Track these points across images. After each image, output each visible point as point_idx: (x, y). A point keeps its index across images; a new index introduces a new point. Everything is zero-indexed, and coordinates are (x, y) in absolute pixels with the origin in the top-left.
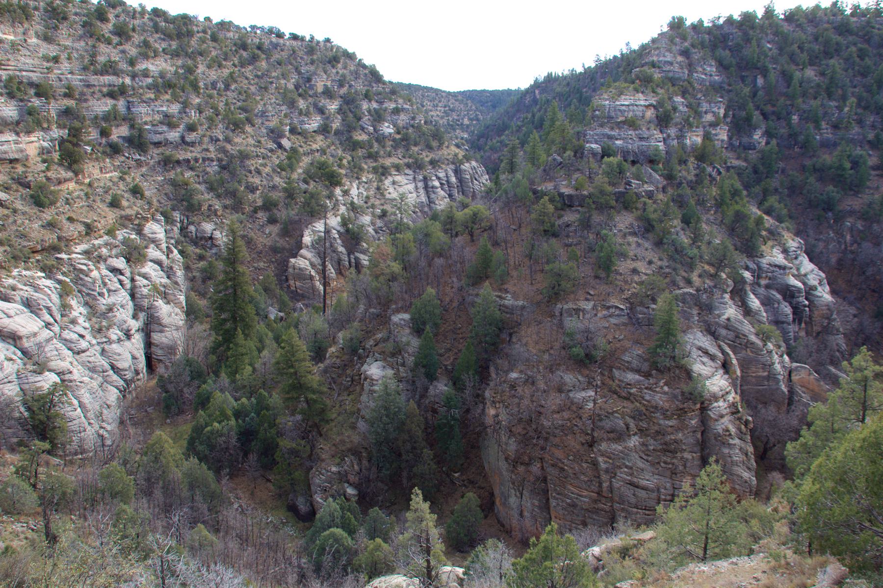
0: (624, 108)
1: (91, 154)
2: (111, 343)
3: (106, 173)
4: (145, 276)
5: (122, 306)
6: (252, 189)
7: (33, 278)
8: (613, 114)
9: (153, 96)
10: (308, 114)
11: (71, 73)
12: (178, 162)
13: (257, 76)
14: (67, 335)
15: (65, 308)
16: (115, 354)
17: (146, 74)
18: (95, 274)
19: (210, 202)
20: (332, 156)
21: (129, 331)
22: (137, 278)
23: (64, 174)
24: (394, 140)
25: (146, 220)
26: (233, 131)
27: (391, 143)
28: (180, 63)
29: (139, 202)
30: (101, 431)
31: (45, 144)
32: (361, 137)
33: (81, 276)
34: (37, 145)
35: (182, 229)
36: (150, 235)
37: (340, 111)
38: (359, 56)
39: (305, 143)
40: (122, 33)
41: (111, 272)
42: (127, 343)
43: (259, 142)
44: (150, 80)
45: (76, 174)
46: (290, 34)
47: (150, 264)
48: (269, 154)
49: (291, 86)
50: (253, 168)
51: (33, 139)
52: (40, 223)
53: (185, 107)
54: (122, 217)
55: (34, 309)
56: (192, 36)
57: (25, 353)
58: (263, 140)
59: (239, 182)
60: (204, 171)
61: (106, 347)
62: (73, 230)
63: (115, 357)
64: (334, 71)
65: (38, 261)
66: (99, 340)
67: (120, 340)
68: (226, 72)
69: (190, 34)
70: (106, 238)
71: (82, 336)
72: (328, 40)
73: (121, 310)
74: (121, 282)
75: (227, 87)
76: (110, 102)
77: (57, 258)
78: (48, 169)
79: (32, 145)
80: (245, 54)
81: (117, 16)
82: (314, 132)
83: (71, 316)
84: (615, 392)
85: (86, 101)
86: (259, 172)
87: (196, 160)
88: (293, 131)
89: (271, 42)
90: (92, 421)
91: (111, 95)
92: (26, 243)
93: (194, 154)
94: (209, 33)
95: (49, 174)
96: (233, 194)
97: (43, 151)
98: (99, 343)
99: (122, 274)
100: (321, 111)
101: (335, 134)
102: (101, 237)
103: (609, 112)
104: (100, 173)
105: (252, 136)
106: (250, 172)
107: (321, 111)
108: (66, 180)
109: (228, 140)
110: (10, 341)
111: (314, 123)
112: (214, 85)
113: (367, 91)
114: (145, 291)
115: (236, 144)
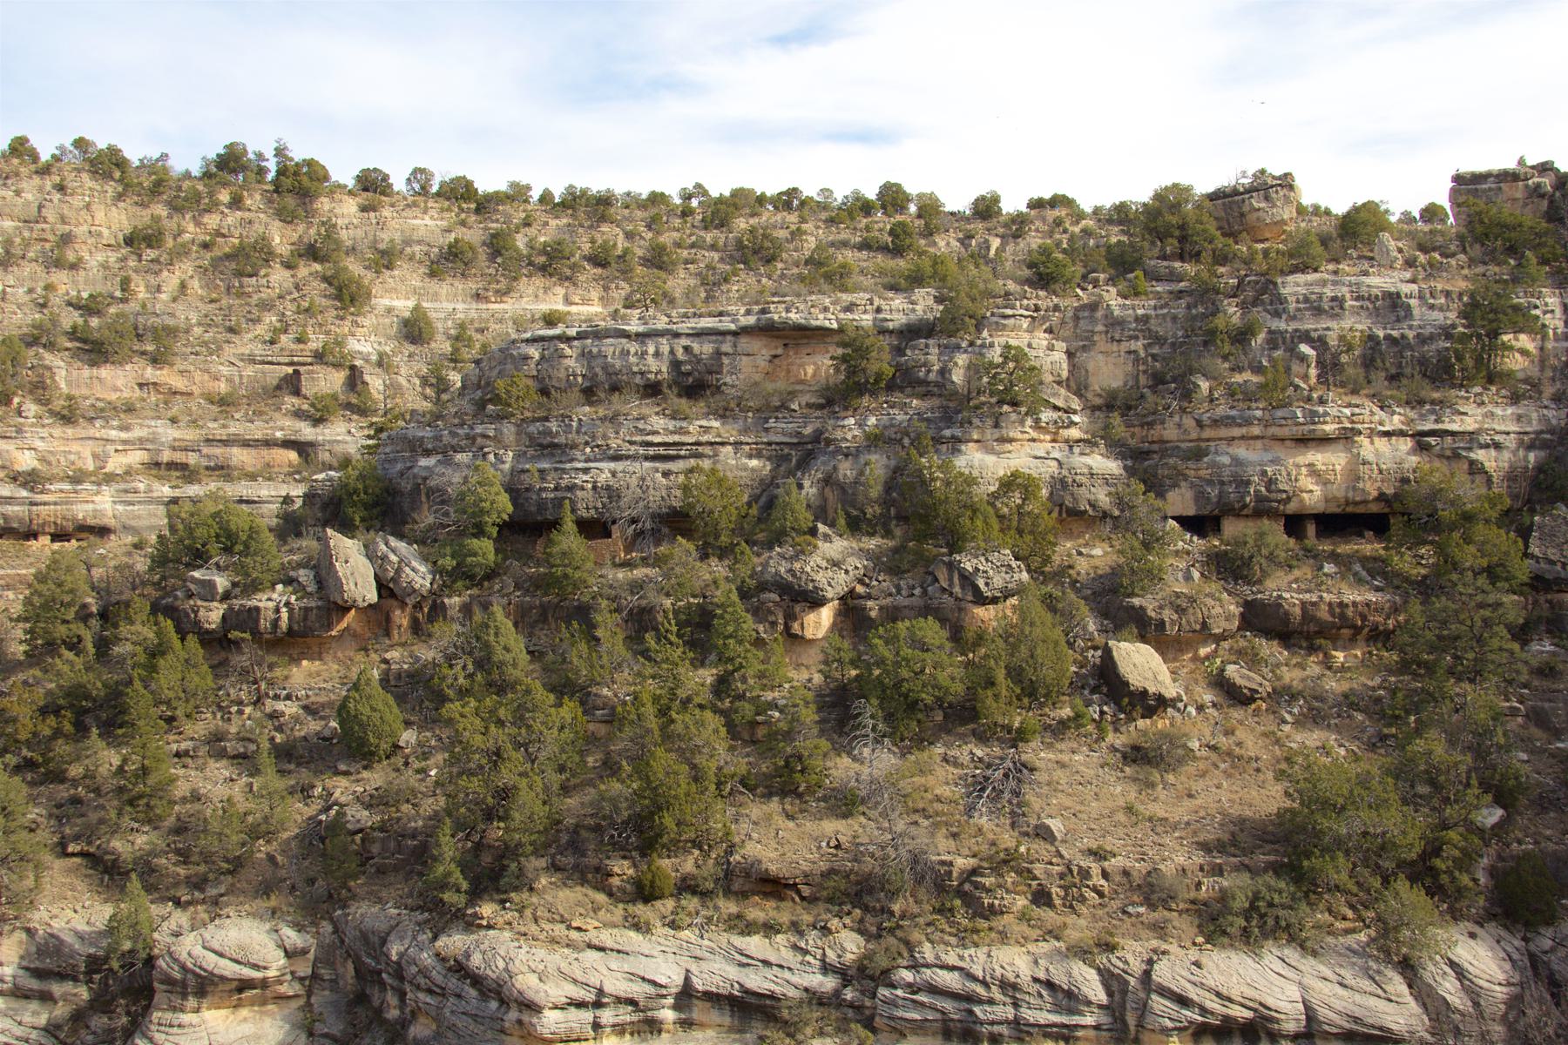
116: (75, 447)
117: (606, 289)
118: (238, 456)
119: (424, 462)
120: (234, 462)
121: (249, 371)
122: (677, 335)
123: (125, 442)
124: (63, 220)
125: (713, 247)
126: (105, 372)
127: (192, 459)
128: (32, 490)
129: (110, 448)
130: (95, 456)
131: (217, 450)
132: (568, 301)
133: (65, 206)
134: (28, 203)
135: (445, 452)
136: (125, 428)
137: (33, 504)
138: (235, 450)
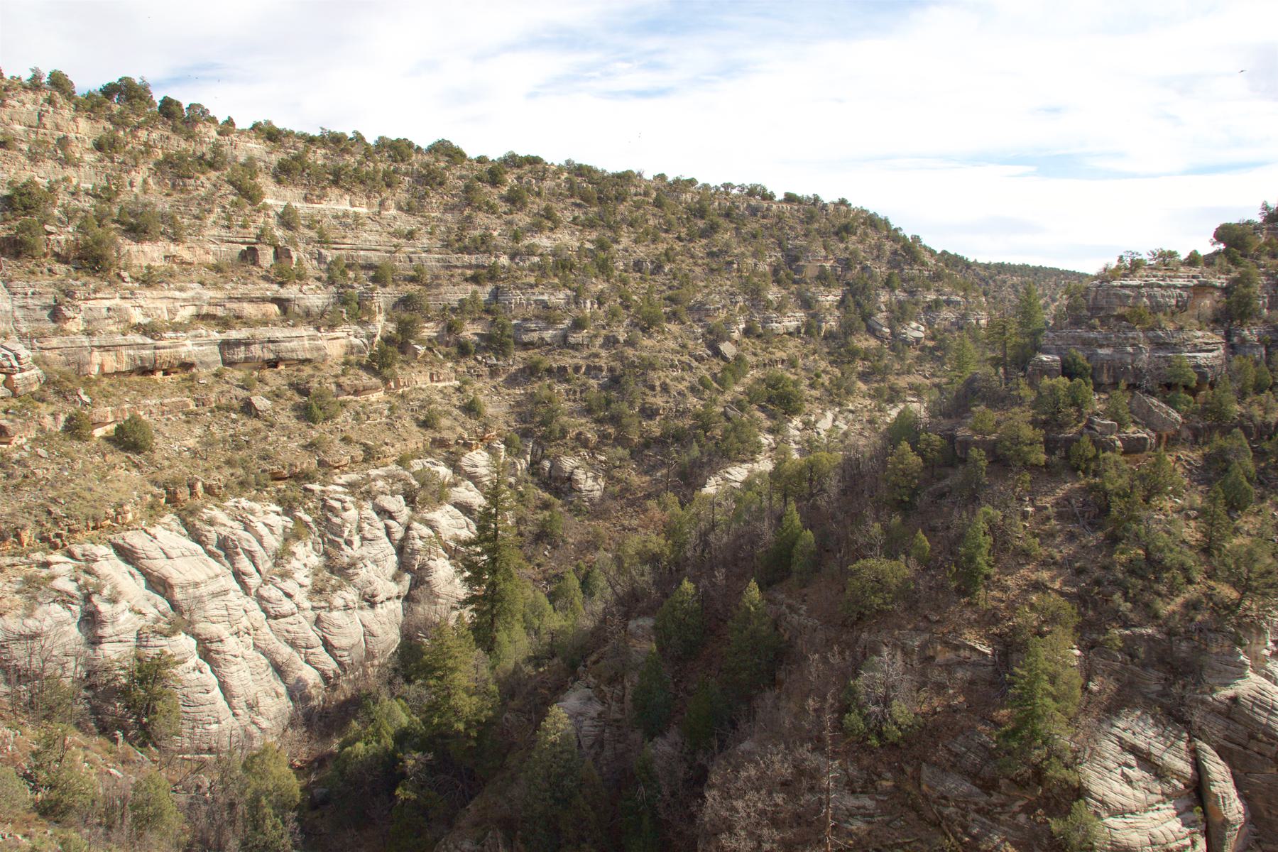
0: (1127, 292)
1: (425, 356)
2: (331, 610)
3: (439, 381)
4: (430, 524)
5: (375, 562)
6: (649, 413)
7: (252, 512)
8: (1103, 303)
9: (532, 280)
10: (780, 308)
11: (428, 251)
12: (549, 371)
13: (711, 255)
14: (271, 592)
15: (280, 557)
16: (333, 625)
17: (531, 251)
18: (352, 514)
19: (581, 429)
20: (806, 369)
21: (373, 596)
22: (415, 525)
23: (366, 379)
24: (923, 349)
25: (468, 446)
26: (644, 330)
27: (918, 352)
28: (594, 235)
29: (472, 423)
30: (253, 729)
31: (357, 341)
32: (863, 342)
33: (329, 514)
34: (344, 342)
35: (532, 464)
36: (468, 469)
37: (842, 303)
38: (894, 224)
39: (765, 350)
40: (514, 199)
41: (378, 514)
42: (368, 614)
43: (684, 346)
44: (536, 259)
45: (386, 381)
46: (787, 194)
47: (449, 507)
48: (695, 364)
49: (764, 267)
50: (658, 383)
51: (338, 334)
52: (302, 442)
53: (577, 297)
54: (434, 440)
55: (230, 551)
56: (624, 200)
57: (174, 606)
58: (690, 344)
59: (631, 404)
60: (584, 385)
61: (323, 613)
62: (340, 453)
63: (332, 629)
64: (842, 246)
65: (279, 490)
66: (315, 604)
67: (347, 607)
68: (662, 247)
69: (620, 198)
70: (393, 467)
71: (289, 596)
72: (843, 202)
73: (370, 566)
74: (388, 528)
75: (658, 269)
76: (471, 287)
77: (306, 489)
78: (344, 374)
79: (337, 343)
80: (701, 224)
81: (519, 178)
82: (790, 334)
83: (288, 567)
84: (914, 807)
85: (439, 286)
86: (665, 388)
87: (577, 369)
88: (747, 332)
89: (749, 205)
90: (239, 711)
91: (475, 279)
92: (268, 467)
93: (576, 360)
94: (654, 195)
95: (342, 380)
96: (615, 420)
97: (351, 349)
98: (314, 608)
99: (392, 517)
100: (806, 303)
101: (825, 338)
102: (386, 465)
103: (1095, 298)
104: (427, 381)
105: (675, 338)
106: (653, 388)
107: (806, 303)
108: (366, 389)
109: (630, 343)
110: (161, 589)
111: (792, 320)
112: (638, 266)
113: (890, 276)
114: (419, 544)
115: (643, 348)
116: (159, 304)
117: (369, 197)
118: (249, 310)
119: (1100, 351)
120: (245, 313)
121: (224, 247)
122: (1175, 287)
123: (185, 300)
124: (58, 127)
125: (406, 174)
126: (147, 247)
127: (220, 312)
128: (152, 338)
129: (178, 304)
130: (169, 311)
131: (235, 305)
132: (352, 205)
133: (59, 117)
134: (30, 113)
135: (1119, 347)
136: (181, 290)
137: (156, 348)
138: (245, 305)
